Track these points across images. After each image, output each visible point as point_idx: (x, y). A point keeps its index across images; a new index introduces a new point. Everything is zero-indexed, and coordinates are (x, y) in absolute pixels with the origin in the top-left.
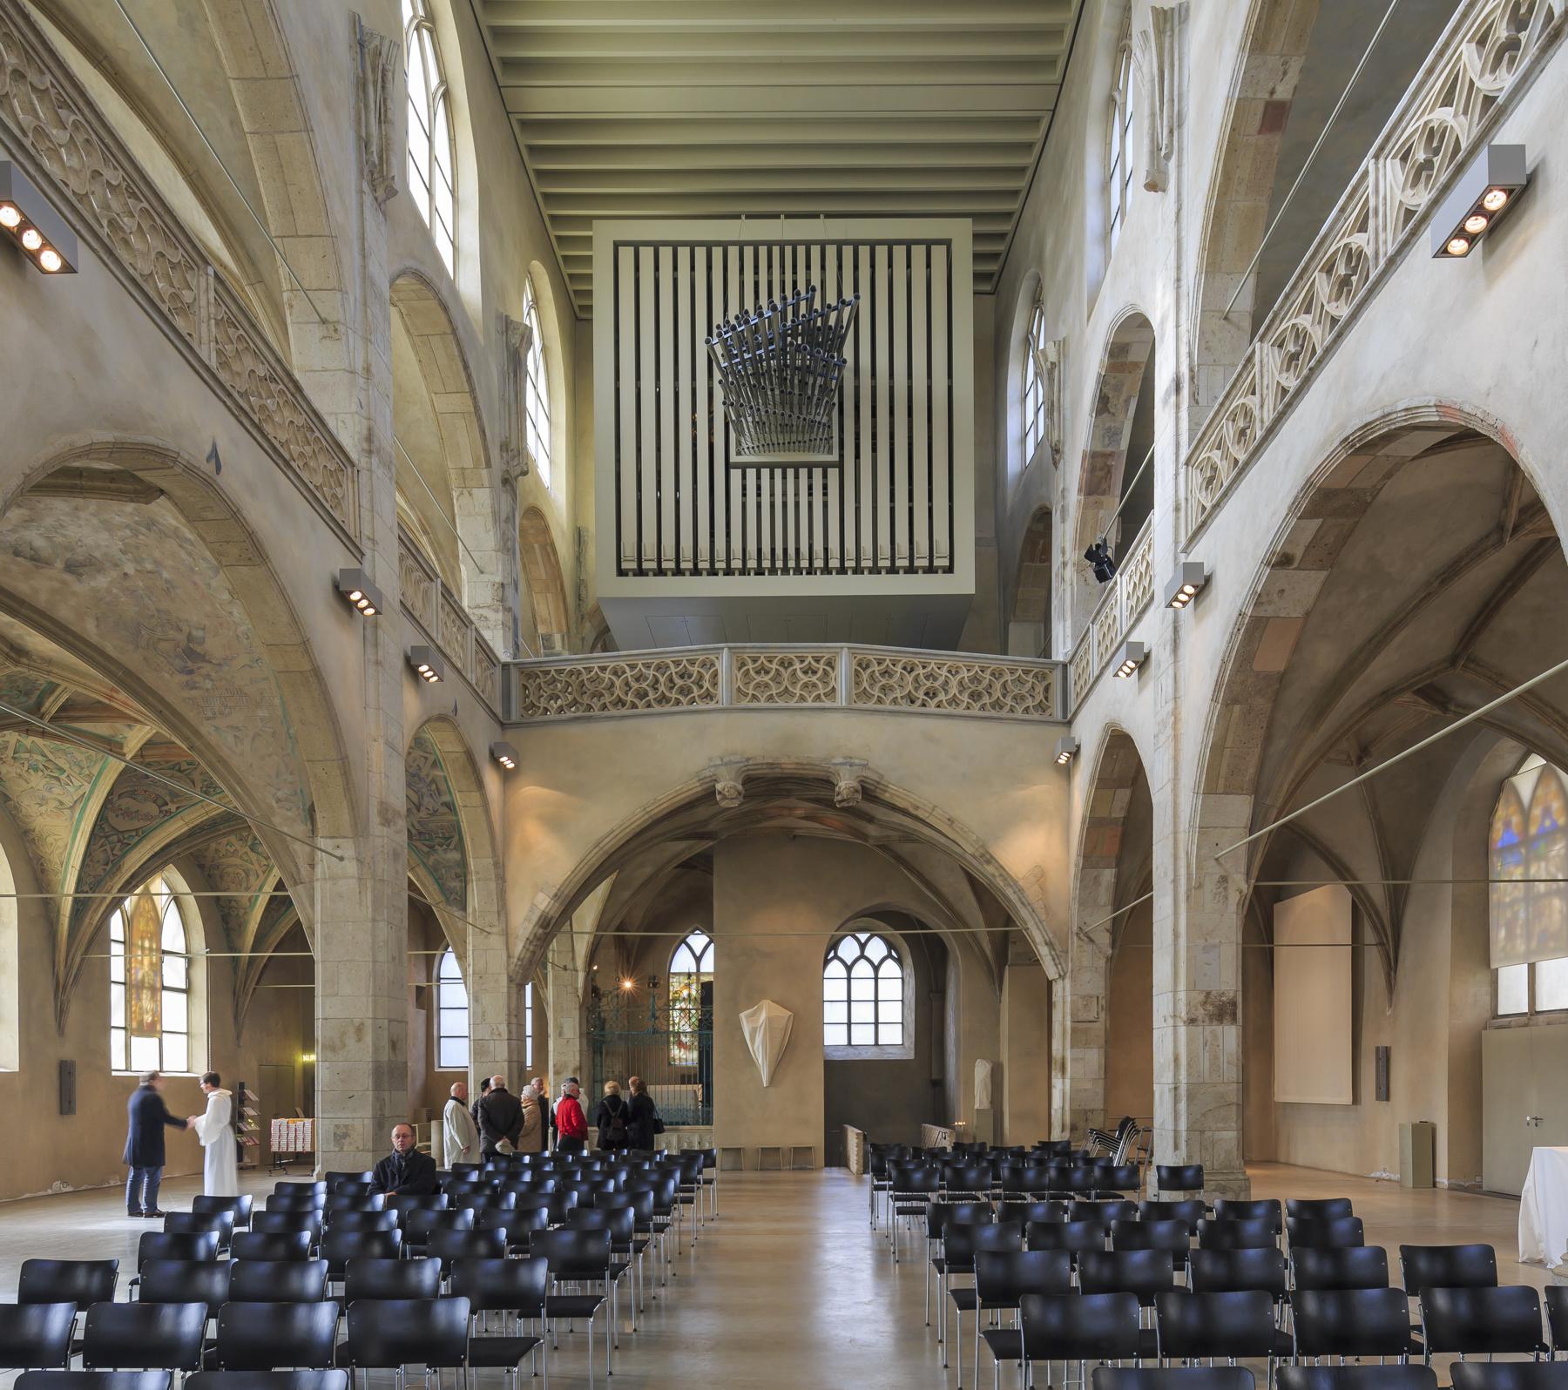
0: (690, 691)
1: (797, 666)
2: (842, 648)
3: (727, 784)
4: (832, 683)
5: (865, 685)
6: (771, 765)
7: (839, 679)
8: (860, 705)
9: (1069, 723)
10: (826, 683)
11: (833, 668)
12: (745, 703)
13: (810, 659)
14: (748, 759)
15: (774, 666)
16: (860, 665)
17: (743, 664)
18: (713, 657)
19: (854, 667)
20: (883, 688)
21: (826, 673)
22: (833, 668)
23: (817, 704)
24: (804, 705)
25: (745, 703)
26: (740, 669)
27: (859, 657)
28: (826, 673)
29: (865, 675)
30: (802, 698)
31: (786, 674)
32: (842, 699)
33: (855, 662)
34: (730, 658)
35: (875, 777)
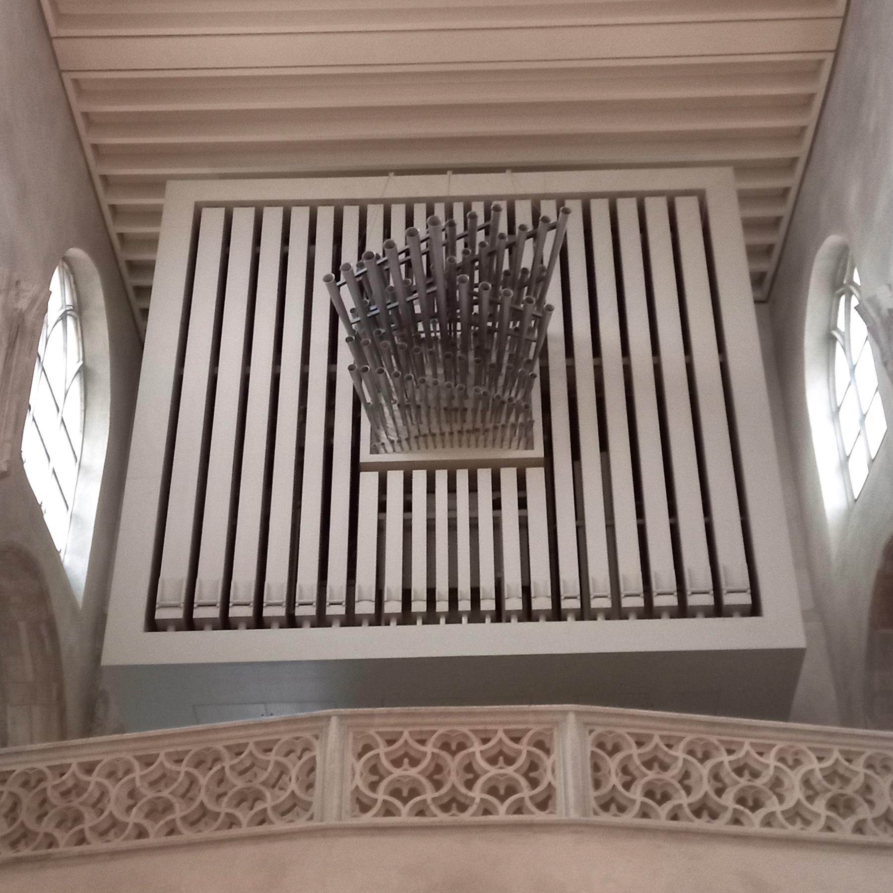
1: (476, 748)
2: (565, 713)
4: (548, 778)
5: (615, 780)
7: (559, 772)
8: (605, 818)
10: (534, 783)
11: (548, 752)
12: (367, 819)
13: (501, 734)
16: (601, 745)
17: (367, 748)
18: (308, 735)
19: (590, 748)
21: (533, 766)
22: (548, 752)
26: (360, 756)
27: (599, 730)
28: (533, 766)
31: (453, 764)
33: (590, 739)
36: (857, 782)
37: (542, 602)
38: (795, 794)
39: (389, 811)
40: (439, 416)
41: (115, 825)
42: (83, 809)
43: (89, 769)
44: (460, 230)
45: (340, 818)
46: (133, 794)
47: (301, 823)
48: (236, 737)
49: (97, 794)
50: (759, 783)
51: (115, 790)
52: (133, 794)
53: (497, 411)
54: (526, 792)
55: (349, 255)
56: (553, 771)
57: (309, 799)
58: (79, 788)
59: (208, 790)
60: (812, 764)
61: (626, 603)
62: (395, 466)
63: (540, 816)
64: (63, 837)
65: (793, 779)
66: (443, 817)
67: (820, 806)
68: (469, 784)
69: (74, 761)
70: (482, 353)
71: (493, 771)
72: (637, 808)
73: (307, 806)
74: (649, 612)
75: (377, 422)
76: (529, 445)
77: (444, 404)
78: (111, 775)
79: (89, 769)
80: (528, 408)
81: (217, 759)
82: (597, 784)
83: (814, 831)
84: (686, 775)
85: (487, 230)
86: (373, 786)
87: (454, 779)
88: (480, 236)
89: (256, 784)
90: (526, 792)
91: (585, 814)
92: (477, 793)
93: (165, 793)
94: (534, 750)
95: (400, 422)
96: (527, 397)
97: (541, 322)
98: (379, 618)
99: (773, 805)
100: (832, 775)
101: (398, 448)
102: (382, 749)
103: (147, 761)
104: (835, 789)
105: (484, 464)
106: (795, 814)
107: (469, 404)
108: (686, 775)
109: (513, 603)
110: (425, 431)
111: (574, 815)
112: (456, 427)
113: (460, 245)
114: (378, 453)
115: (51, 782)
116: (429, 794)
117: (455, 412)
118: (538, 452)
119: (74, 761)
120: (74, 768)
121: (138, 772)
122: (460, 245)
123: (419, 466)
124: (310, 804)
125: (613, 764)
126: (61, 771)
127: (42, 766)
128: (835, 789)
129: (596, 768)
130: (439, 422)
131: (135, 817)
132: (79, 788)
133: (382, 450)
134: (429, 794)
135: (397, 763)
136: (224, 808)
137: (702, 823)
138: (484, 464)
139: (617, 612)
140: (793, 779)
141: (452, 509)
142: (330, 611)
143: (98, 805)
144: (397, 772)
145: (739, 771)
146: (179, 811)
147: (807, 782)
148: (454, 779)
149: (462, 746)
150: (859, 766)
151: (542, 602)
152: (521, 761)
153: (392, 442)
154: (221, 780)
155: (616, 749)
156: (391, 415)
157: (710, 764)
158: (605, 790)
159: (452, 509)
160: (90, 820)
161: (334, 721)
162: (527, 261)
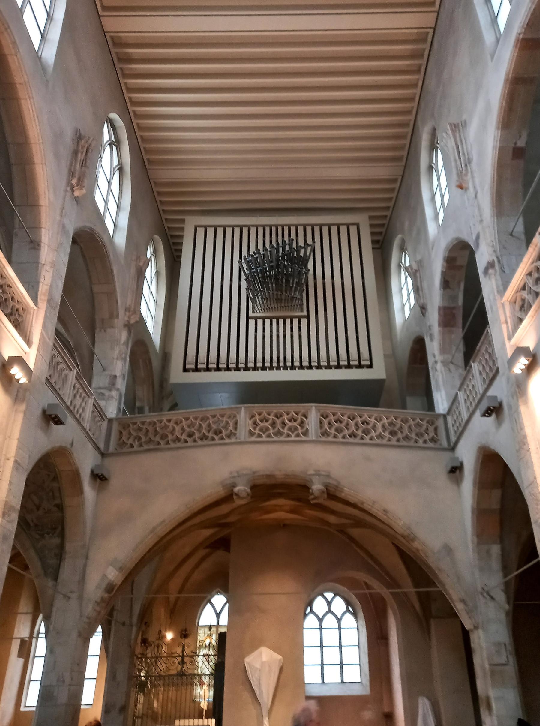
0: (221, 432)
1: (285, 417)
2: (312, 406)
3: (242, 488)
5: (326, 427)
6: (268, 476)
8: (323, 439)
9: (453, 449)
10: (302, 427)
11: (306, 418)
12: (253, 439)
14: (254, 473)
15: (271, 417)
16: (322, 416)
17: (253, 416)
18: (235, 413)
19: (319, 416)
20: (337, 430)
22: (306, 418)
23: (297, 439)
24: (289, 439)
25: (253, 439)
26: (251, 419)
27: (322, 411)
29: (326, 422)
30: (289, 436)
31: (278, 421)
32: (312, 435)
33: (319, 414)
34: (246, 413)
35: (334, 483)
36: (398, 426)
37: (306, 363)
38: (380, 430)
39: (260, 436)
40: (273, 301)
41: (178, 439)
42: (168, 434)
43: (169, 421)
44: (281, 245)
45: (245, 438)
46: (183, 429)
47: (233, 440)
48: (213, 413)
49: (172, 429)
50: (369, 427)
51: (177, 428)
52: (183, 429)
53: (292, 300)
54: (300, 431)
55: (245, 253)
56: (308, 424)
57: (235, 432)
58: (166, 427)
59: (205, 428)
60: (385, 421)
61: (332, 364)
62: (260, 318)
63: (304, 438)
64: (162, 442)
65: (379, 425)
66: (275, 438)
67: (387, 434)
68: (283, 428)
69: (165, 419)
70: (287, 281)
71: (290, 424)
72: (333, 435)
73: (235, 434)
74: (339, 367)
75: (254, 302)
76: (302, 311)
77: (275, 297)
78: (176, 423)
79: (169, 421)
80: (302, 300)
81: (208, 418)
82: (321, 427)
83: (385, 442)
84: (348, 424)
85: (289, 245)
86: (255, 429)
87: (279, 426)
88: (287, 248)
89: (220, 427)
90: (300, 431)
91: (317, 437)
92: (286, 431)
93: (193, 429)
94: (303, 417)
95: (261, 302)
96: (301, 295)
97: (307, 274)
98: (255, 368)
99: (373, 434)
100: (391, 424)
101: (261, 311)
102: (257, 417)
103: (187, 419)
104: (391, 428)
105: (288, 317)
106: (380, 436)
107: (283, 297)
108: (348, 424)
109: (297, 364)
110: (269, 306)
111: (314, 438)
112: (279, 305)
113: (281, 249)
114: (255, 313)
115: (158, 425)
116: (271, 431)
117: (278, 300)
118: (305, 313)
119: (165, 419)
120: (165, 421)
121: (184, 422)
122: (281, 249)
123: (267, 318)
124: (236, 434)
125: (326, 422)
126: (161, 421)
127: (155, 420)
128: (391, 428)
129: (321, 423)
130: (274, 303)
131: (184, 437)
132: (166, 427)
133: (256, 312)
134: (271, 431)
135: (262, 421)
136: (211, 435)
137: (351, 440)
138: (288, 317)
139: (329, 367)
140: (379, 425)
141: (278, 331)
142: (240, 366)
143: (172, 432)
144: (262, 424)
145: (363, 423)
146: (197, 435)
147: (383, 426)
148: (279, 426)
149: (281, 416)
150: (399, 422)
151: (306, 363)
152: (299, 421)
153: (259, 310)
154: (209, 425)
155: (327, 416)
156: (259, 300)
157: (354, 421)
158: (323, 430)
159: (278, 331)
160: (170, 437)
161: (243, 409)
162: (302, 254)
